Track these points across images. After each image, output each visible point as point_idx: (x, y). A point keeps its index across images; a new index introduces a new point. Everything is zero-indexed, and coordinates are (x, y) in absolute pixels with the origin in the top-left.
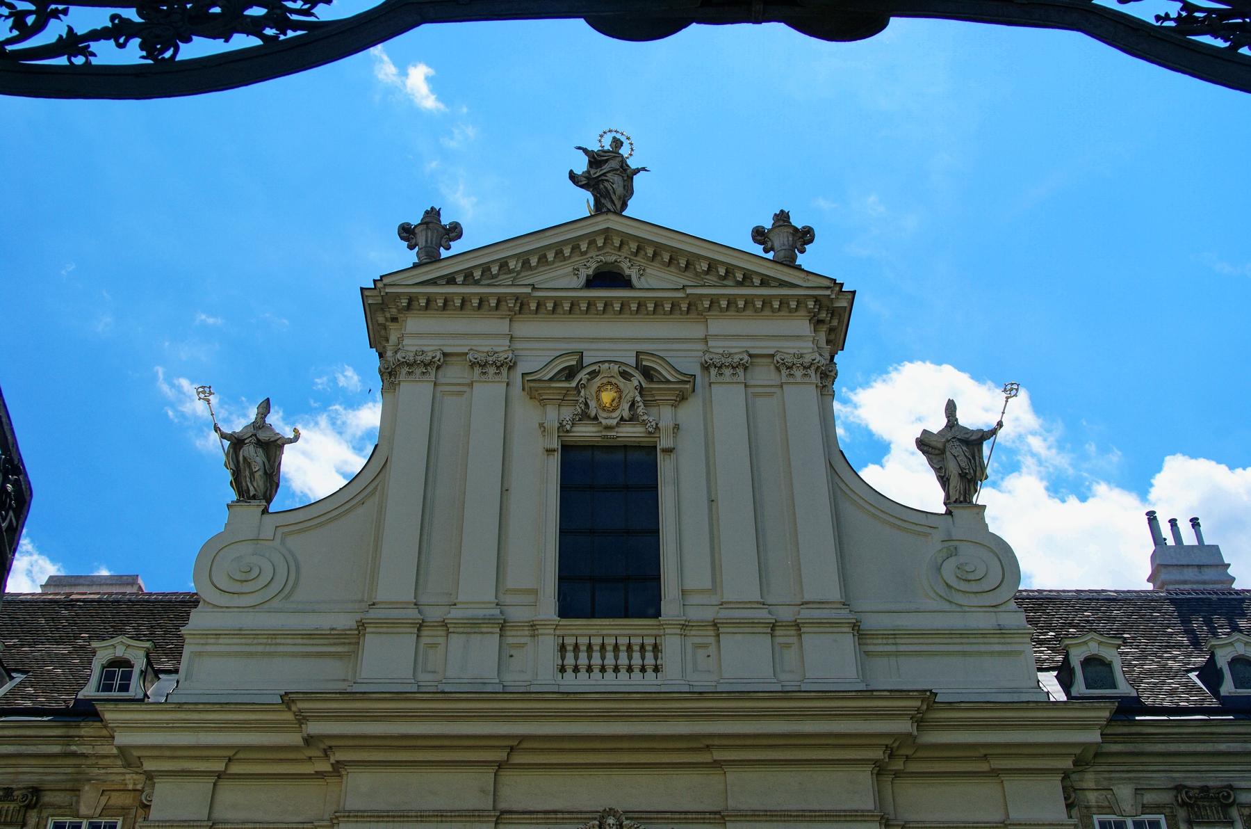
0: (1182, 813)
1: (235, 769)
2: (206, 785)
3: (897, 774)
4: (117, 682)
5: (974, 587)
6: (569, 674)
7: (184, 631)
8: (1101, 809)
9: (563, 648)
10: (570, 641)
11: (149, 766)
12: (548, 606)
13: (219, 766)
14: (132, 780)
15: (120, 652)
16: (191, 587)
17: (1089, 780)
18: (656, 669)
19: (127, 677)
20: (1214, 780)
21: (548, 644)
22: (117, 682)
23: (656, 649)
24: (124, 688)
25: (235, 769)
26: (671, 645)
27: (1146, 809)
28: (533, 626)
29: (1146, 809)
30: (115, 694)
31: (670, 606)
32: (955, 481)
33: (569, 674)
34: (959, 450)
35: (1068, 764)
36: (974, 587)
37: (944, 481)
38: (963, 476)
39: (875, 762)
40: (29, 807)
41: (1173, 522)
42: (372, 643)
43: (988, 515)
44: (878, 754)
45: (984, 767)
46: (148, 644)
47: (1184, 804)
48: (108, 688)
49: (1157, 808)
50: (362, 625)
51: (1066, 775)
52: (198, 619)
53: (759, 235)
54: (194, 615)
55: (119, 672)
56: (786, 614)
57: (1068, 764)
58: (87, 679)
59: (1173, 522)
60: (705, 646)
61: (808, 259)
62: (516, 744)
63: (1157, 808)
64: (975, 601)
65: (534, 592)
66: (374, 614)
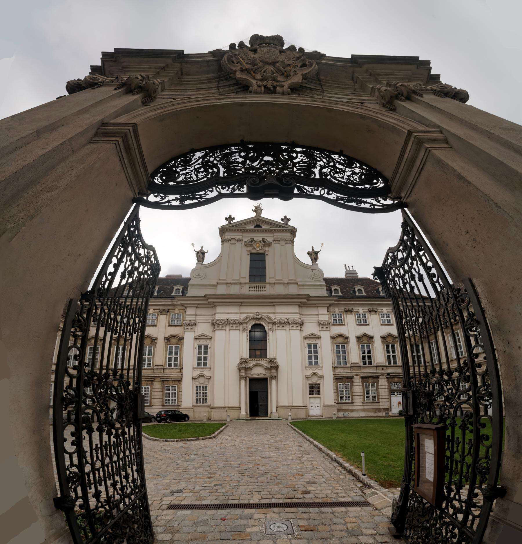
0: (345, 313)
1: (199, 306)
2: (195, 308)
3: (302, 307)
4: (178, 292)
5: (316, 277)
6: (251, 292)
7: (188, 284)
8: (333, 312)
9: (250, 287)
10: (251, 286)
11: (185, 306)
12: (247, 281)
13: (197, 306)
14: (183, 308)
15: (178, 288)
16: (190, 277)
17: (331, 308)
18: (265, 291)
19: (179, 292)
20: (350, 308)
21: (247, 287)
22: (178, 292)
23: (265, 287)
24: (179, 294)
25: (199, 306)
26: (268, 287)
27: (339, 312)
28: (245, 284)
29: (339, 312)
30: (177, 295)
31: (267, 281)
32: (313, 260)
33: (251, 292)
34: (313, 254)
35: (328, 305)
36: (316, 277)
37: (312, 260)
38: (315, 259)
39: (299, 305)
40: (167, 312)
41: (349, 266)
42: (219, 286)
43: (319, 265)
44: (299, 304)
45: (315, 306)
46: (183, 286)
47: (346, 311)
48: (176, 294)
49: (341, 312)
50: (217, 283)
51: (328, 307)
52: (191, 282)
53: (282, 219)
54: (190, 281)
55: (178, 291)
56: (286, 282)
57: (328, 305)
58: (173, 292)
59: (349, 266)
60: (273, 287)
61: (290, 223)
62: (242, 303)
63: (341, 312)
64: (317, 279)
65: (245, 278)
66: (219, 281)
